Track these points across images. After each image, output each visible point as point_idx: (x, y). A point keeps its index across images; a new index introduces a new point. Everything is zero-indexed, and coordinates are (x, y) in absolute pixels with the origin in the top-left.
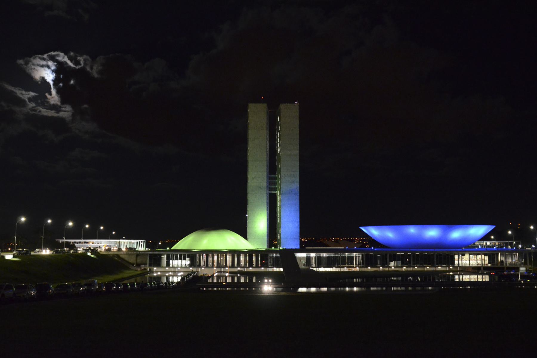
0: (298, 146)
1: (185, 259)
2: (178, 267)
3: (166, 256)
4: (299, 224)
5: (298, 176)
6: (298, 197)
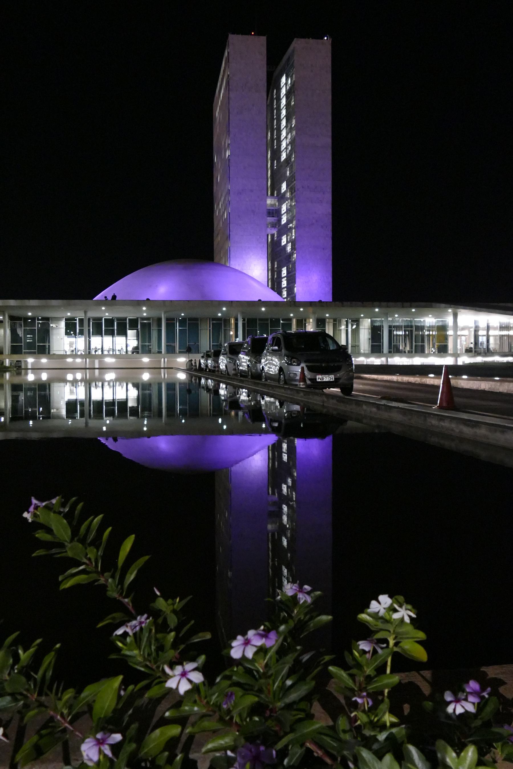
0: (330, 128)
1: (125, 334)
2: (103, 355)
3: (63, 324)
4: (331, 286)
5: (329, 190)
6: (330, 234)
